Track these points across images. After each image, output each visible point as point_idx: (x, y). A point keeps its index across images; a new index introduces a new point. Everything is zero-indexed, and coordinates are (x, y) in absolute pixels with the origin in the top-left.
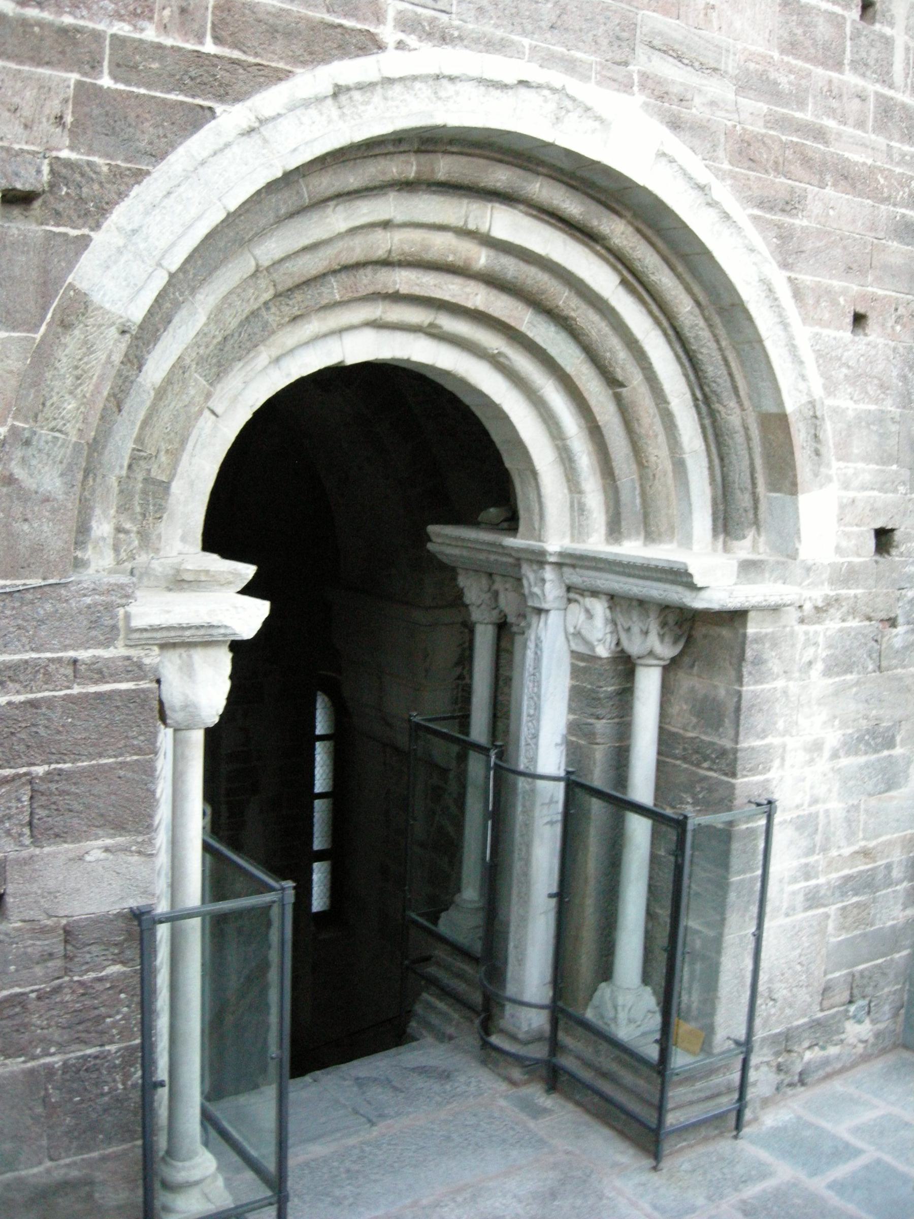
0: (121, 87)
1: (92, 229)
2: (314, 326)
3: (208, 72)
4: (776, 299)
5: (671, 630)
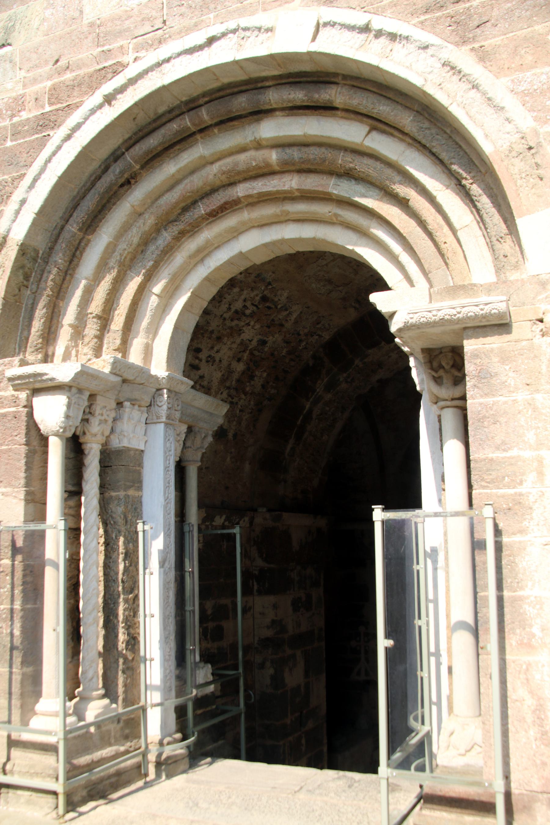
0: (14, 143)
1: (4, 206)
2: (206, 235)
3: (47, 120)
5: (446, 372)
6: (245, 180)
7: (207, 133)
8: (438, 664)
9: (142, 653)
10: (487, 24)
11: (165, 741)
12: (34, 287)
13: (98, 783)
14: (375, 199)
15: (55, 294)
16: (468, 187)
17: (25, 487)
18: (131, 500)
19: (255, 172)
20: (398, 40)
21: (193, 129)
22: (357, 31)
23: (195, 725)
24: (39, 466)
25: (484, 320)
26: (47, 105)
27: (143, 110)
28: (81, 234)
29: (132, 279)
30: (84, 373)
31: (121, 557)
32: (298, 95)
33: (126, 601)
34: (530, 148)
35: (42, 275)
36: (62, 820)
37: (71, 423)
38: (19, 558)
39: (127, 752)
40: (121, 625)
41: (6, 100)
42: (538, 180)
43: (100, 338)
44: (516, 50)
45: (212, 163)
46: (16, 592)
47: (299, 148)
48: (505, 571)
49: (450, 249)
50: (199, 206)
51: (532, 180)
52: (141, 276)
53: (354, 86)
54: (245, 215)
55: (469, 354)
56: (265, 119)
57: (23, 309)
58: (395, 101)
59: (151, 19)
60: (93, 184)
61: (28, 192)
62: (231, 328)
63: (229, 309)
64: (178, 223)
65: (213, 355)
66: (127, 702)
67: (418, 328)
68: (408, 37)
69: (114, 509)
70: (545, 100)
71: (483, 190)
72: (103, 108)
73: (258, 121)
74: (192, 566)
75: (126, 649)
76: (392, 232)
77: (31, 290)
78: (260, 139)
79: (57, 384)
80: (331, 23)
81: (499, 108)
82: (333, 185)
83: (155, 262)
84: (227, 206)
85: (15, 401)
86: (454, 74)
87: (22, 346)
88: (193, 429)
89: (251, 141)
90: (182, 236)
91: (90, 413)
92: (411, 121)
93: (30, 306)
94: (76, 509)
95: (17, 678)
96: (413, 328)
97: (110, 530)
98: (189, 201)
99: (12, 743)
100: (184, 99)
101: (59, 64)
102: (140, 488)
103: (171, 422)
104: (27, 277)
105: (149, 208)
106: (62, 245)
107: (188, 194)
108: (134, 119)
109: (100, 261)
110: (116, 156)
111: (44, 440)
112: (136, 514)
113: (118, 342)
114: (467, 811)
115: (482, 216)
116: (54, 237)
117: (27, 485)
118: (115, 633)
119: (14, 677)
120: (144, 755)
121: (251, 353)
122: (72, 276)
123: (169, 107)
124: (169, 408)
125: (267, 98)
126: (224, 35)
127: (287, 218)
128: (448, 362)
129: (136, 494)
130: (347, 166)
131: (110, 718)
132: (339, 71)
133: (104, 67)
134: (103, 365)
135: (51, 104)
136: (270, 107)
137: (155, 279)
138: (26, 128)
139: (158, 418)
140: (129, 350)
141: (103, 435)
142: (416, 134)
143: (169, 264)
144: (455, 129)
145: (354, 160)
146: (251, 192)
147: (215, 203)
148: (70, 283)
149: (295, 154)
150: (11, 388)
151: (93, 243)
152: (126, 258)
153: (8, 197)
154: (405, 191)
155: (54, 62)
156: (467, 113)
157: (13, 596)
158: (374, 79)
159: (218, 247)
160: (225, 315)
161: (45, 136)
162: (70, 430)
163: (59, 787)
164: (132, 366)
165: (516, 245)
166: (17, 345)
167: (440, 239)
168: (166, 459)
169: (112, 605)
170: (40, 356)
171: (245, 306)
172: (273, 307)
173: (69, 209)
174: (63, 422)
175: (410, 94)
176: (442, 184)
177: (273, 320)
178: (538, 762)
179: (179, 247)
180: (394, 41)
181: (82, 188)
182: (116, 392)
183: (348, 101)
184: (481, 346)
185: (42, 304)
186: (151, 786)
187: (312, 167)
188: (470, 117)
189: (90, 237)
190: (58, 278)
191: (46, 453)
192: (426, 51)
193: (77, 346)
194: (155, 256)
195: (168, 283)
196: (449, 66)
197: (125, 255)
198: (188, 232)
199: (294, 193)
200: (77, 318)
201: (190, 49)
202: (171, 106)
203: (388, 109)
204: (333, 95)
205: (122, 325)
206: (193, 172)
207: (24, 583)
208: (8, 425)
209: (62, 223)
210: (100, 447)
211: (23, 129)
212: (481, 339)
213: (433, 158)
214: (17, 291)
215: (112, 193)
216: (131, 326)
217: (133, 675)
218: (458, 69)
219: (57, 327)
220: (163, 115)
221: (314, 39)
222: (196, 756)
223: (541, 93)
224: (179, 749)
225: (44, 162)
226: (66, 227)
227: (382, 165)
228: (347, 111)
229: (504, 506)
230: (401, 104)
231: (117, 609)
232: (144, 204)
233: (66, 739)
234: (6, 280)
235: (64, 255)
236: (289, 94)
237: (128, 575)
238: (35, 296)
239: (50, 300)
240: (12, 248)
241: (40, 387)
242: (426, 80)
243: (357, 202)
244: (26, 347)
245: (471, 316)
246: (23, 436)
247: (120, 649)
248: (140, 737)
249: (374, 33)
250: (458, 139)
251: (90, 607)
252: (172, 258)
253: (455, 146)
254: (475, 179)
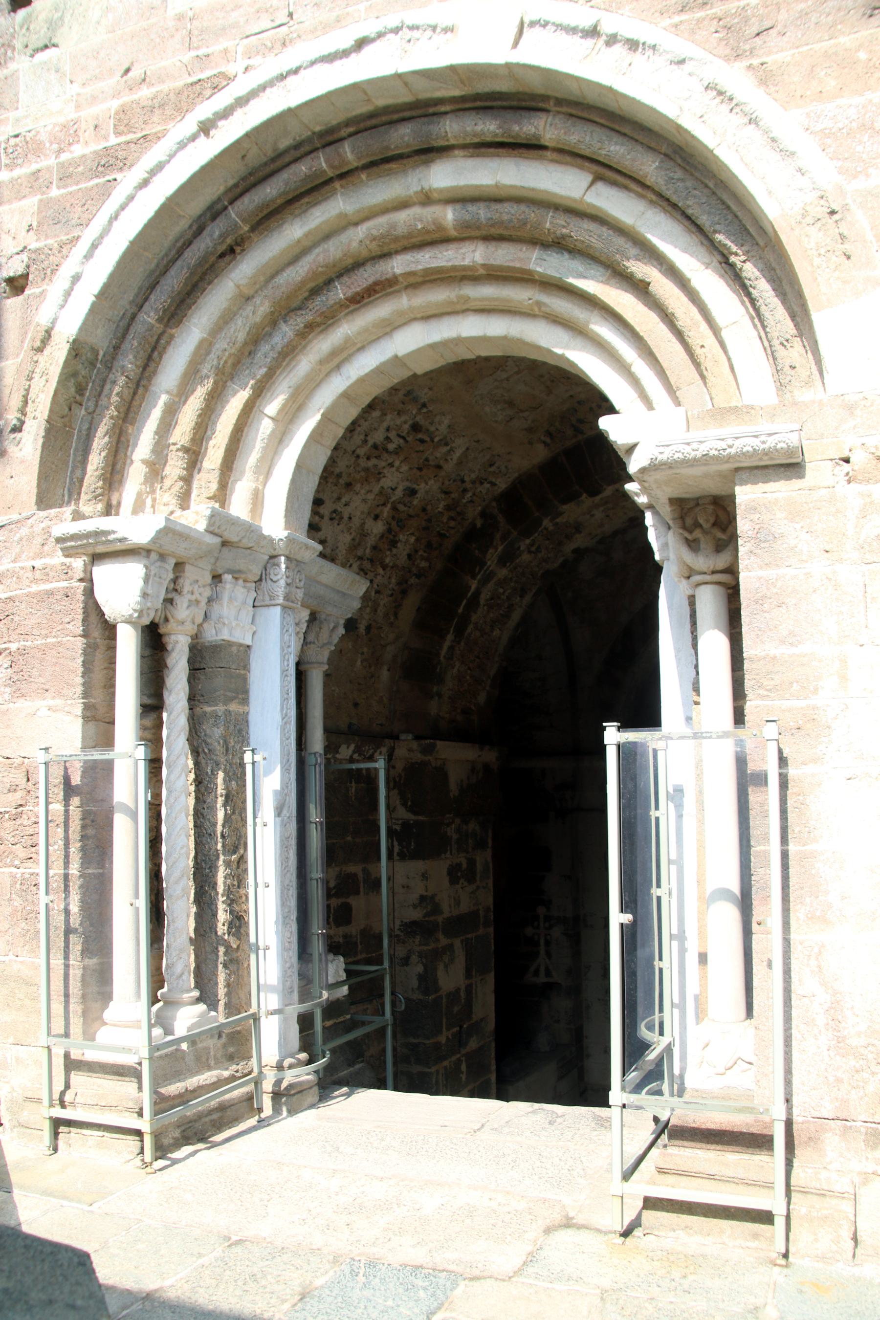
0: (63, 191)
1: (48, 285)
2: (345, 330)
3: (112, 157)
4: (731, 99)
5: (705, 532)
6: (405, 249)
7: (350, 179)
8: (682, 951)
9: (252, 939)
10: (771, 31)
11: (286, 1064)
12: (91, 404)
13: (195, 1121)
14: (598, 281)
15: (122, 415)
16: (739, 267)
17: (83, 698)
18: (233, 718)
19: (419, 239)
20: (640, 50)
21: (330, 174)
22: (580, 34)
23: (325, 1041)
24: (102, 667)
25: (766, 458)
26: (112, 136)
27: (257, 144)
28: (159, 327)
29: (235, 393)
30: (169, 531)
31: (220, 801)
32: (488, 127)
33: (228, 864)
34: (833, 213)
35: (102, 387)
36: (149, 1170)
37: (149, 604)
38: (75, 801)
39: (233, 1078)
40: (221, 899)
41: (49, 128)
42: (843, 258)
43: (187, 480)
44: (812, 71)
45: (356, 224)
46: (72, 850)
47: (487, 203)
48: (791, 816)
49: (709, 356)
50: (336, 287)
51: (834, 258)
52: (248, 389)
53: (571, 115)
54: (404, 302)
55: (743, 507)
56: (438, 161)
57: (75, 437)
58: (632, 138)
59: (271, 10)
60: (180, 253)
61: (83, 263)
62: (367, 470)
63: (365, 442)
64: (304, 312)
65: (339, 509)
66: (232, 1008)
67: (670, 467)
68: (655, 46)
69: (208, 732)
70: (854, 144)
71: (761, 271)
72: (197, 141)
73: (427, 163)
74: (315, 815)
75: (229, 934)
76: (622, 330)
77: (86, 409)
78: (430, 190)
79: (128, 547)
80: (542, 22)
81: (788, 153)
82: (536, 259)
83: (270, 369)
84: (377, 288)
85: (67, 571)
86: (722, 102)
87: (74, 491)
88: (318, 616)
89: (416, 193)
90: (311, 329)
91: (176, 590)
92: (656, 168)
93: (84, 433)
94: (153, 731)
95: (76, 973)
96: (664, 467)
97: (203, 762)
98: (321, 280)
99: (71, 1065)
100: (318, 129)
101: (130, 74)
102: (245, 701)
103: (291, 604)
104: (81, 390)
105: (261, 289)
106: (132, 342)
107: (320, 269)
108: (243, 157)
109: (188, 366)
110: (214, 212)
111: (110, 630)
112: (240, 739)
113: (214, 486)
114: (731, 1148)
115: (759, 308)
116: (121, 331)
117: (86, 695)
118: (212, 910)
119: (71, 972)
120: (257, 1082)
121: (394, 508)
122: (146, 389)
123: (294, 140)
124: (288, 584)
125: (443, 130)
126: (380, 35)
127: (464, 307)
128: (710, 518)
129: (241, 709)
130: (558, 232)
131: (211, 1029)
132: (550, 93)
133: (200, 81)
134: (196, 518)
135: (118, 134)
136: (447, 143)
137: (269, 394)
138: (81, 169)
139: (272, 598)
140: (230, 498)
141: (194, 623)
142: (664, 188)
143: (290, 372)
144: (722, 181)
145: (568, 224)
146: (413, 268)
147: (361, 283)
148: (143, 398)
149: (481, 212)
150: (60, 553)
151: (177, 340)
152: (226, 362)
153: (53, 272)
154: (644, 271)
155: (122, 72)
156: (742, 159)
157: (67, 856)
158: (602, 106)
159: (362, 348)
160: (358, 451)
161: (110, 181)
162: (148, 615)
163: (144, 1125)
164: (235, 522)
165: (809, 352)
166: (66, 490)
167: (694, 341)
168: (284, 658)
169: (207, 871)
170: (100, 507)
171: (387, 439)
172: (428, 439)
173: (144, 289)
174: (138, 603)
175: (656, 128)
176: (699, 261)
177: (427, 460)
178: (831, 1079)
179: (305, 347)
180: (634, 51)
181: (163, 259)
182: (213, 560)
183: (563, 137)
184: (761, 495)
185: (102, 430)
186: (269, 1125)
187: (506, 233)
188: (746, 165)
189: (174, 331)
190: (126, 391)
191: (112, 648)
192: (681, 66)
193: (153, 492)
194: (269, 360)
195: (287, 401)
196: (716, 90)
197: (224, 358)
198: (319, 325)
199: (478, 270)
200: (154, 451)
201: (329, 55)
202: (298, 138)
203: (622, 150)
204: (541, 128)
205: (220, 461)
206: (327, 237)
207: (83, 838)
208: (57, 607)
209: (132, 310)
210: (190, 640)
211: (76, 170)
213: (687, 223)
214: (67, 409)
215: (207, 266)
216: (233, 463)
217: (238, 970)
218: (728, 94)
219: (125, 464)
220: (286, 151)
221: (516, 44)
222: (329, 1084)
223: (848, 134)
224: (305, 1075)
225: (107, 219)
226: (138, 316)
227: (611, 232)
228: (561, 151)
229: (792, 724)
230: (642, 143)
231: (215, 876)
232: (255, 283)
233: (151, 1058)
234: (52, 393)
235: (135, 357)
236: (476, 125)
237: (230, 827)
238: (93, 418)
239: (114, 424)
240: (60, 346)
241: (102, 551)
242: (681, 109)
243: (571, 284)
244: (79, 494)
246: (79, 623)
247: (219, 933)
248: (250, 1057)
249: (604, 38)
250: (725, 197)
251: (177, 874)
252: (293, 363)
253: (721, 207)
254: (750, 254)
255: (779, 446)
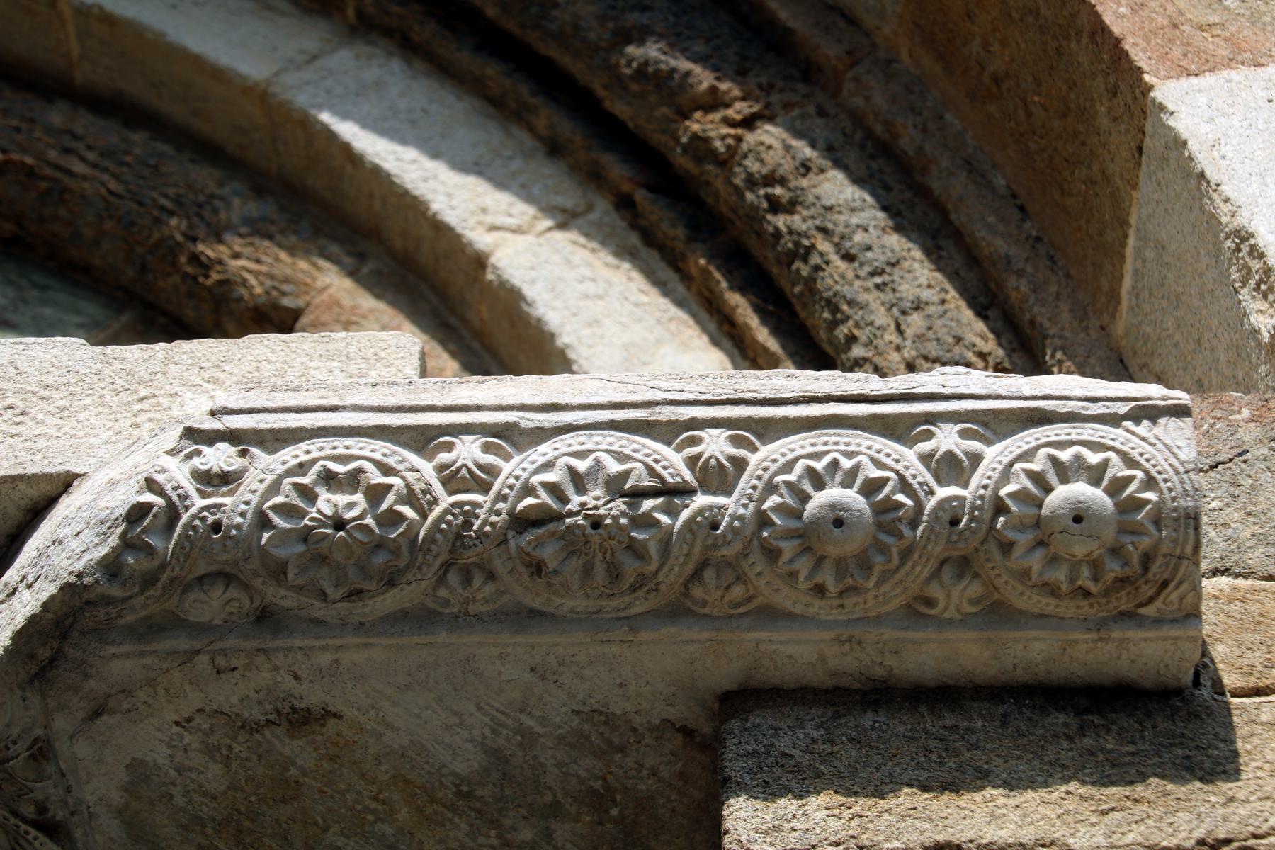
25: (957, 596)
67: (266, 619)
96: (210, 605)
176: (529, 199)
212: (907, 798)
245: (838, 519)
255: (1063, 494)
